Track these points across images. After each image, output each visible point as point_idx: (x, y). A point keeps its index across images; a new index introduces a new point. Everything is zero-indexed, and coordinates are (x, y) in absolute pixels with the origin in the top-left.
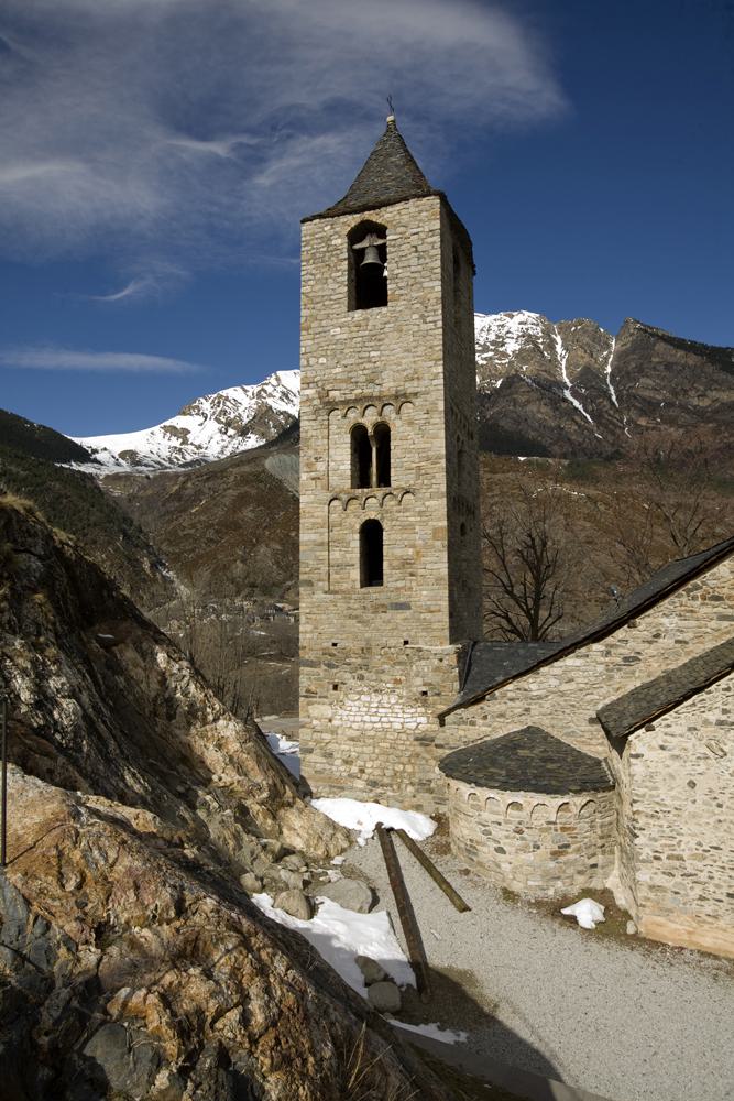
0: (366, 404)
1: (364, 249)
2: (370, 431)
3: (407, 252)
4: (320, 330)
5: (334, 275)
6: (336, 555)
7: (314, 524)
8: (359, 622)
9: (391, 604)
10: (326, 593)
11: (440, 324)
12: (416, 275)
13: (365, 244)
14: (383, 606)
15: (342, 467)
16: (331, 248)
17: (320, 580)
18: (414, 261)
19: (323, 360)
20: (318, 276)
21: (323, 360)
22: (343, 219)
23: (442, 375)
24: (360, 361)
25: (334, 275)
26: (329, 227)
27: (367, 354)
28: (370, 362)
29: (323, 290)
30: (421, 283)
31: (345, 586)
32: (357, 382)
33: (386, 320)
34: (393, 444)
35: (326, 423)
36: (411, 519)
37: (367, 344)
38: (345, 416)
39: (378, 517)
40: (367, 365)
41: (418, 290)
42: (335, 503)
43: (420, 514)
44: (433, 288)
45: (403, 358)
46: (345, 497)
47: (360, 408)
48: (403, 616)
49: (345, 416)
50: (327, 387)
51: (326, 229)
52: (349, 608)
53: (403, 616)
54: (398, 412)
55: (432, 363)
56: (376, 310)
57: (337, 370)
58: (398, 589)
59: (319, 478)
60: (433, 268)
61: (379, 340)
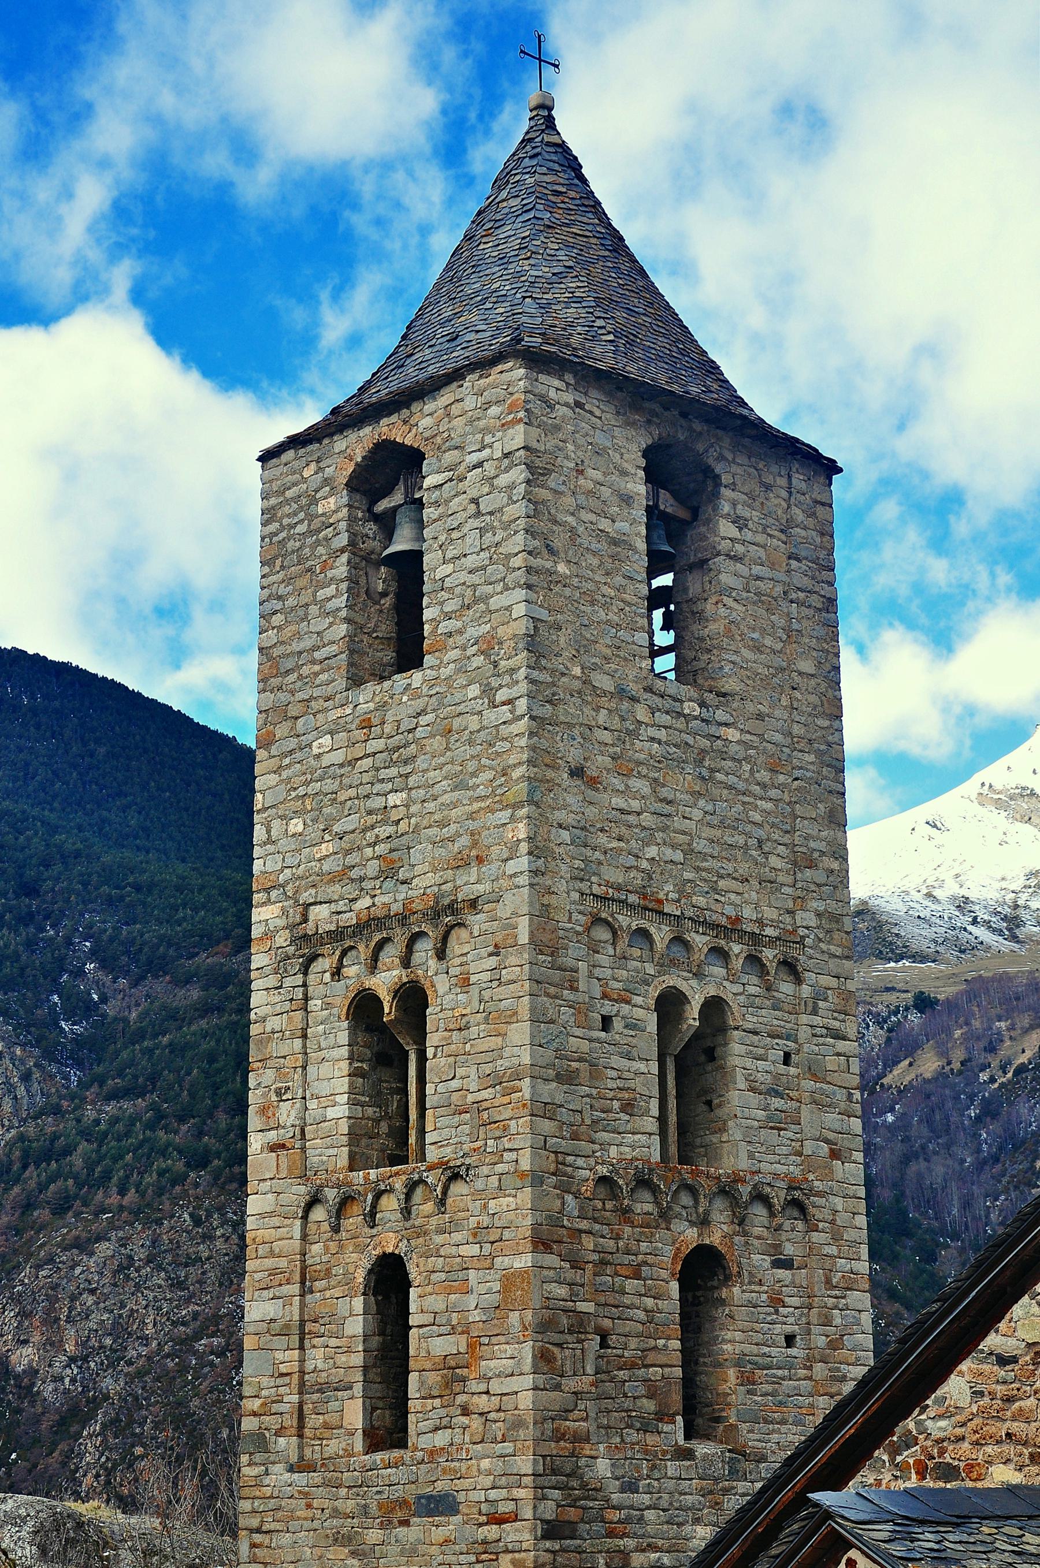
0: (377, 937)
1: (395, 510)
2: (389, 1009)
3: (461, 517)
4: (293, 743)
5: (321, 594)
6: (316, 1358)
7: (273, 1272)
8: (353, 1554)
9: (420, 1497)
10: (291, 1469)
11: (522, 705)
12: (475, 579)
13: (397, 498)
14: (403, 1503)
15: (331, 1113)
16: (316, 523)
17: (278, 1433)
18: (472, 539)
19: (296, 825)
20: (291, 602)
21: (296, 825)
22: (340, 444)
23: (524, 847)
24: (371, 819)
25: (321, 594)
26: (313, 466)
27: (377, 803)
28: (384, 822)
29: (298, 636)
30: (485, 599)
31: (334, 1447)
32: (362, 879)
33: (419, 704)
34: (432, 1040)
35: (299, 993)
36: (464, 1250)
37: (383, 774)
38: (337, 973)
39: (402, 1249)
40: (390, 830)
41: (477, 621)
42: (319, 1214)
43: (477, 1234)
44: (508, 609)
45: (454, 805)
46: (331, 1194)
47: (363, 951)
48: (439, 1534)
49: (337, 973)
50: (306, 896)
51: (306, 474)
52: (336, 1513)
53: (439, 1534)
54: (441, 954)
55: (504, 816)
56: (400, 680)
57: (326, 849)
58: (433, 1453)
59: (283, 1146)
60: (508, 556)
61: (406, 762)
